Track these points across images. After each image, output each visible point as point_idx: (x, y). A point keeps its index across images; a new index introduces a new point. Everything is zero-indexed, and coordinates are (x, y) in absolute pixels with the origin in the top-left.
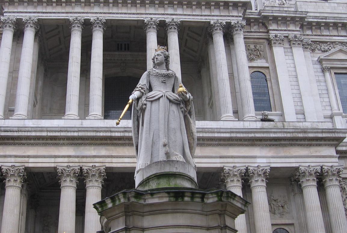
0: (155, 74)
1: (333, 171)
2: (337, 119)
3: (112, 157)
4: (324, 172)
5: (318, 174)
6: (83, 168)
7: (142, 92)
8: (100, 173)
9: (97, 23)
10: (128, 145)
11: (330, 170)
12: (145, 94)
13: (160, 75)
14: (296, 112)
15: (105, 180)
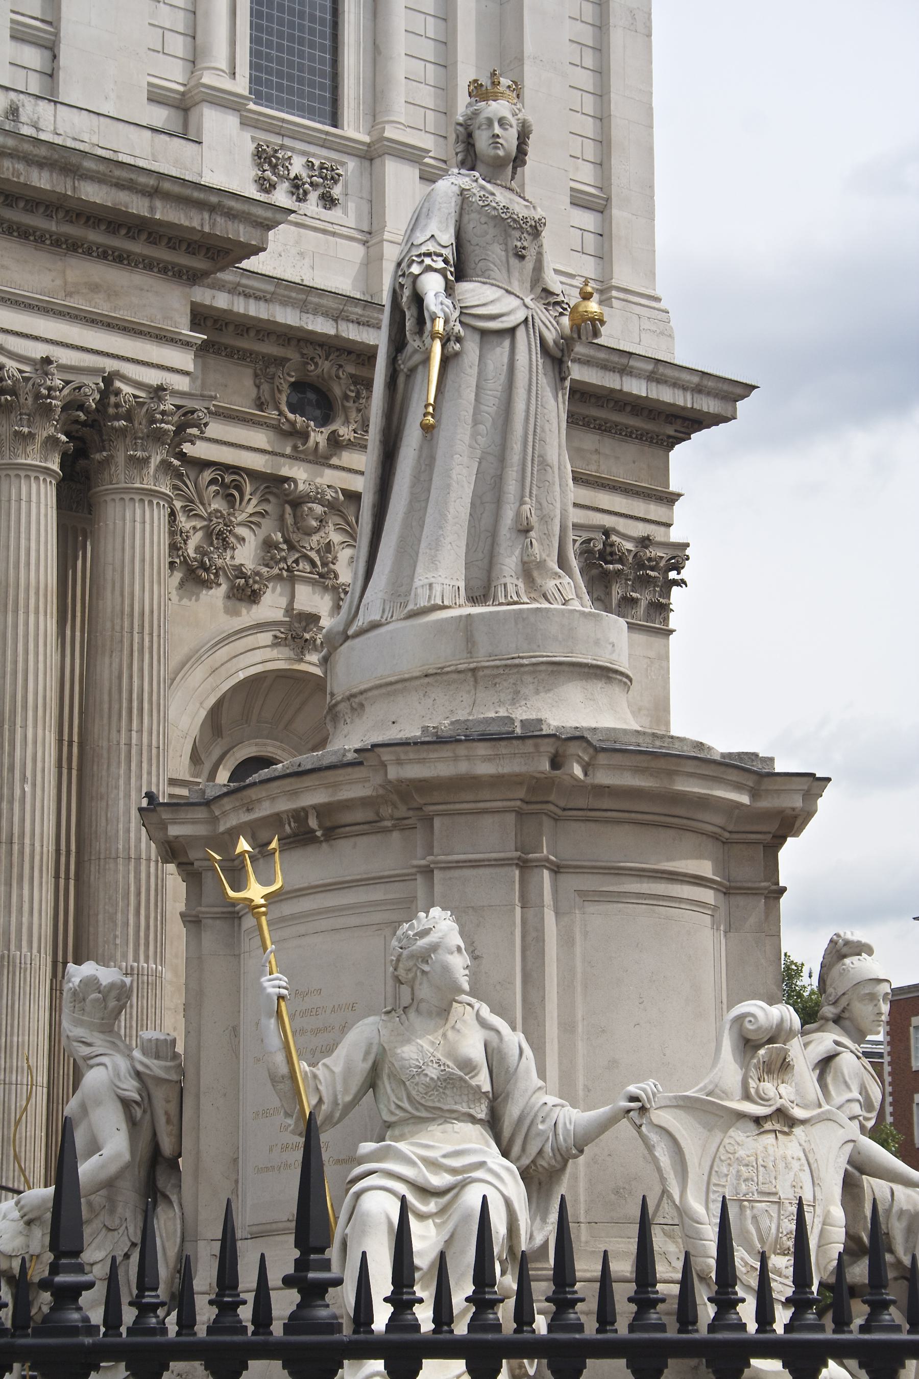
0: (494, 213)
1: (159, 416)
2: (217, 124)
4: (111, 411)
5: (82, 416)
11: (144, 403)
13: (514, 220)
14: (13, 21)
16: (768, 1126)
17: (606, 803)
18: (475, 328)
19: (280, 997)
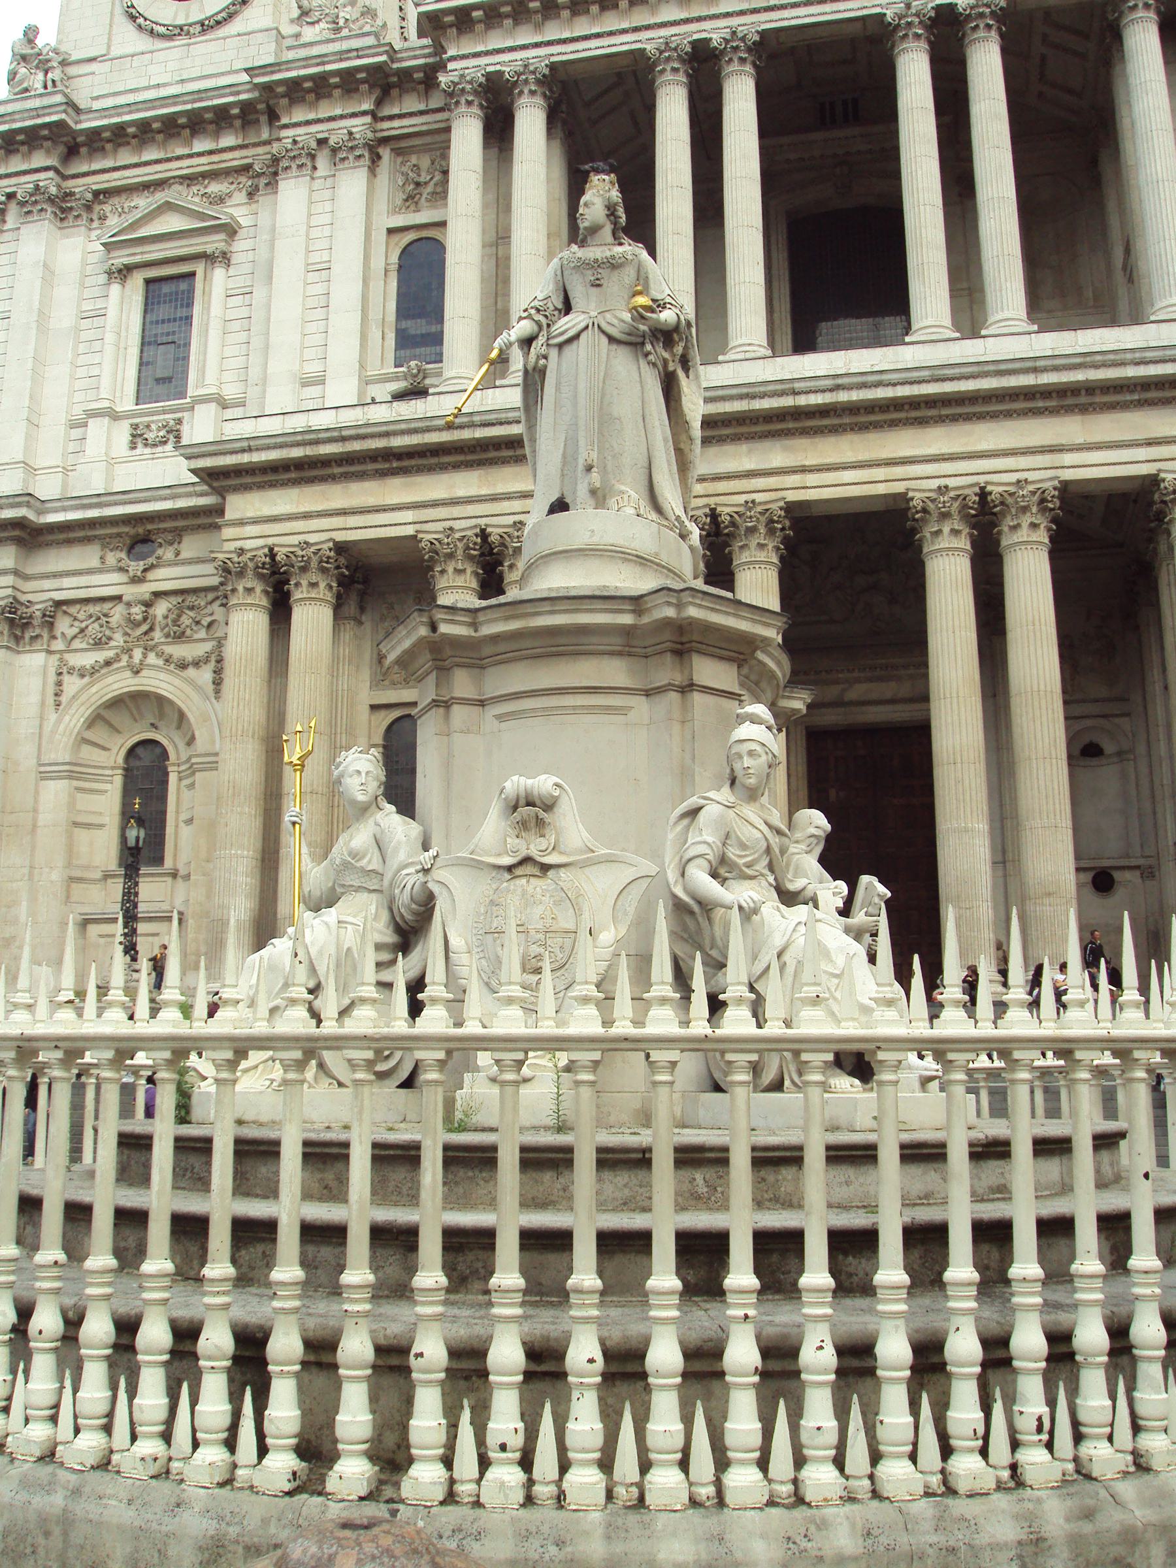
3: (804, 470)
6: (719, 509)
7: (536, 322)
8: (772, 521)
9: (732, 47)
10: (852, 429)
12: (549, 326)
15: (786, 540)
16: (519, 871)
17: (502, 647)
18: (555, 345)
19: (294, 823)
